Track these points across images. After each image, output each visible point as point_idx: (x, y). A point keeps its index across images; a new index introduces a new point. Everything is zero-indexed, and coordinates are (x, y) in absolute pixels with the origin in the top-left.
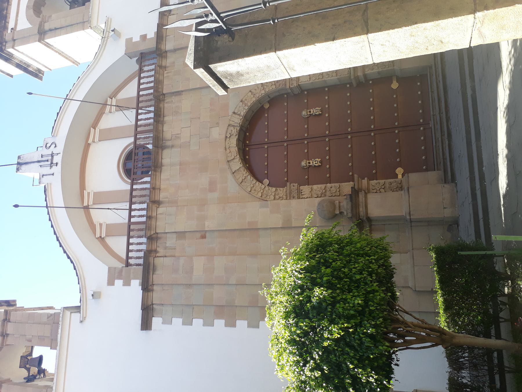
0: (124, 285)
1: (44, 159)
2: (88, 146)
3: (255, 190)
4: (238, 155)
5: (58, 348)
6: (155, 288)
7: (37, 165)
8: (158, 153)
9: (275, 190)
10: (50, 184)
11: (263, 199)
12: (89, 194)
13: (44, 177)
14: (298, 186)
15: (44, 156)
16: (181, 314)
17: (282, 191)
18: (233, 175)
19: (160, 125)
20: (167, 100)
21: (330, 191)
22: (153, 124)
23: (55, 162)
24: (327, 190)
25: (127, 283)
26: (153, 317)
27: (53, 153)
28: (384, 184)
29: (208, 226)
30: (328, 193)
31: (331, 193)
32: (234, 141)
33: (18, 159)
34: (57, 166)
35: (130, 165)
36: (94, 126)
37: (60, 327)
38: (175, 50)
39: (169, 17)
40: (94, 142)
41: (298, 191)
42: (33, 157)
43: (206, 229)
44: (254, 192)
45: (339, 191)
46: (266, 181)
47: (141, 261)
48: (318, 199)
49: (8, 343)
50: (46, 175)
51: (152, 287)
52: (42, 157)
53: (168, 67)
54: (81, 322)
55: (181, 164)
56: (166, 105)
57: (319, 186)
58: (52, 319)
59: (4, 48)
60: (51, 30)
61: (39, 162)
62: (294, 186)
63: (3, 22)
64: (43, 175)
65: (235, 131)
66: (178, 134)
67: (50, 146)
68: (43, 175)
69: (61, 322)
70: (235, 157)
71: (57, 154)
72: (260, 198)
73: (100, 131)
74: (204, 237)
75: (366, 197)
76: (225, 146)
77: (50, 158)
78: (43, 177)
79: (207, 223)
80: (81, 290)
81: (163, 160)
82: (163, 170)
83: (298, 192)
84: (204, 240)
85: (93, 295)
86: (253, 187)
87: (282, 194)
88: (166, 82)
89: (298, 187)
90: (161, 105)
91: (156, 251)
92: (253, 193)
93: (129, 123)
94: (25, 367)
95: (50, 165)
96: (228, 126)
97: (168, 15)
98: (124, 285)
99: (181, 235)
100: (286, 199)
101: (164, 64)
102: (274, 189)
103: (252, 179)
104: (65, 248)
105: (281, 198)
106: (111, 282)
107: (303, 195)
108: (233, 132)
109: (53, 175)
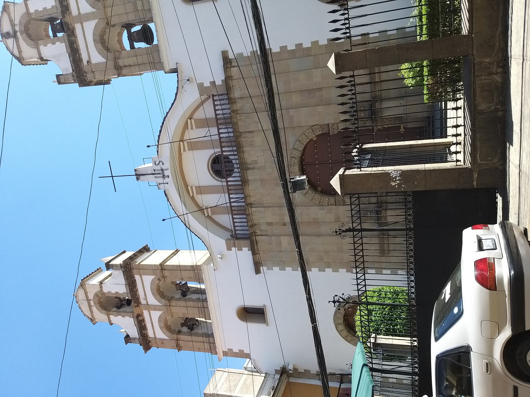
1: (156, 172)
3: (315, 199)
11: (321, 205)
12: (191, 187)
16: (278, 265)
23: (166, 174)
27: (162, 168)
37: (203, 274)
38: (241, 98)
39: (231, 68)
40: (184, 150)
42: (147, 171)
52: (154, 171)
53: (239, 110)
55: (261, 180)
59: (86, 78)
60: (125, 66)
63: (77, 55)
64: (160, 184)
72: (319, 204)
74: (284, 224)
77: (160, 172)
80: (211, 253)
81: (248, 177)
82: (249, 184)
86: (313, 197)
88: (240, 123)
90: (240, 140)
91: (255, 232)
97: (230, 66)
99: (270, 224)
100: (336, 205)
101: (235, 108)
106: (229, 249)
107: (346, 203)
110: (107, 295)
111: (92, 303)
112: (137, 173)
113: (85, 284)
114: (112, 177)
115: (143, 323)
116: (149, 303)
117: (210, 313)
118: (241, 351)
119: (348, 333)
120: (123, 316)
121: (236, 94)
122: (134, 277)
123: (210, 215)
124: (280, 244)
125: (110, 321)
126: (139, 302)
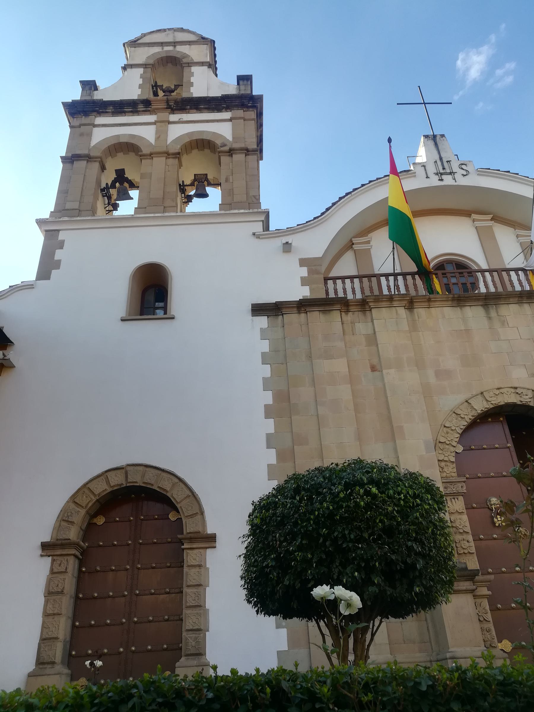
0: (302, 278)
1: (446, 165)
2: (467, 214)
3: (447, 433)
4: (494, 406)
5: (223, 212)
6: (303, 315)
7: (437, 157)
8: (478, 300)
9: (452, 461)
10: (415, 176)
11: (438, 444)
13: (423, 167)
14: (463, 493)
15: (449, 164)
16: (274, 350)
17: (451, 470)
18: (464, 401)
19: (516, 299)
21: (462, 539)
22: (514, 291)
23: (444, 177)
24: (463, 535)
25: (304, 282)
26: (268, 317)
28: (486, 621)
29: (389, 373)
31: (459, 542)
33: (440, 135)
34: (439, 180)
35: (449, 268)
36: (495, 219)
41: (455, 493)
43: (385, 372)
44: (445, 432)
45: (464, 553)
46: (460, 449)
47: (332, 295)
49: (222, 158)
50: (425, 170)
51: (303, 312)
52: (447, 162)
54: (254, 234)
57: (467, 524)
58: (253, 202)
61: (441, 159)
62: (462, 487)
66: (508, 323)
67: (462, 169)
68: (424, 166)
69: (252, 211)
70: (489, 403)
71: (455, 179)
72: (438, 441)
73: (491, 227)
74: (373, 369)
75: (466, 591)
76: (502, 387)
77: (448, 171)
78: (422, 166)
79: (392, 371)
80: (292, 229)
81: (469, 307)
82: (454, 308)
83: (454, 493)
84: (370, 369)
85: (287, 243)
86: (452, 430)
87: (448, 471)
89: (461, 493)
91: (347, 311)
92: (443, 430)
93: (506, 262)
94: (195, 180)
95: (439, 172)
98: (302, 278)
100: (442, 478)
102: (453, 459)
103: (462, 427)
104: (339, 203)
106: (303, 262)
107: (451, 501)
108: (525, 397)
109: (427, 178)
110: (186, 70)
111: (170, 48)
112: (438, 138)
113: (207, 44)
114: (425, 103)
115: (131, 110)
116: (171, 126)
117: (157, 215)
118: (57, 265)
119: (97, 498)
120: (140, 86)
122: (228, 108)
123: (355, 247)
124: (328, 355)
125: (131, 66)
126: (176, 110)
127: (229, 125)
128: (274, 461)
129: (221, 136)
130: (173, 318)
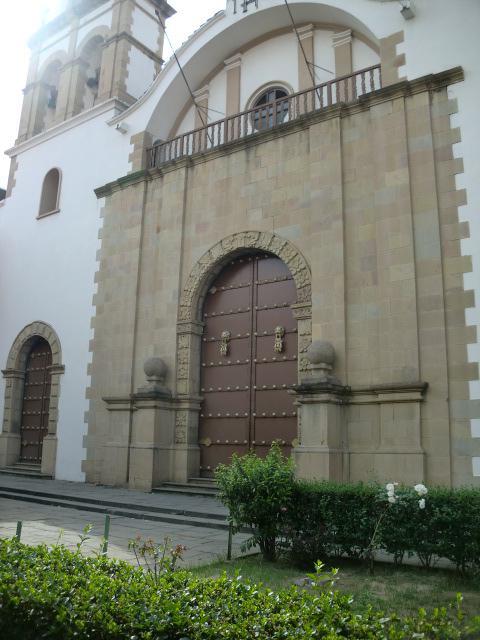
10: (225, 16)
12: (240, 59)
20: (304, 134)
25: (132, 158)
30: (181, 366)
32: (239, 244)
36: (317, 26)
48: (174, 356)
56: (298, 135)
65: (248, 244)
74: (158, 230)
88: (324, 125)
90: (296, 129)
91: (151, 180)
96: (260, 230)
100: (179, 320)
101: (352, 112)
105: (180, 314)
106: (134, 140)
121: (378, 110)
127: (110, 14)
128: (94, 314)
129: (104, 27)
130: (59, 212)
